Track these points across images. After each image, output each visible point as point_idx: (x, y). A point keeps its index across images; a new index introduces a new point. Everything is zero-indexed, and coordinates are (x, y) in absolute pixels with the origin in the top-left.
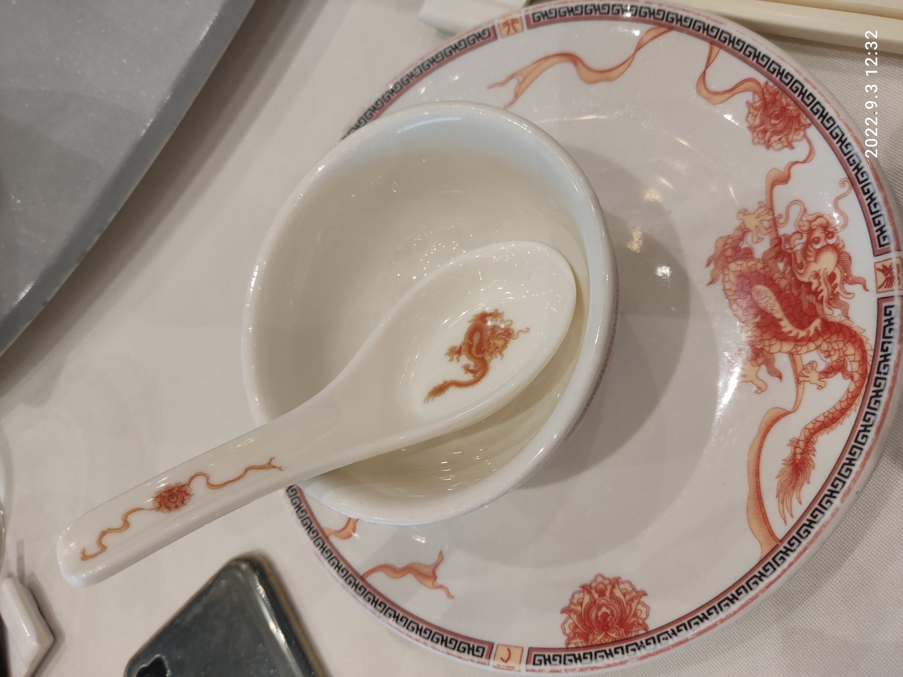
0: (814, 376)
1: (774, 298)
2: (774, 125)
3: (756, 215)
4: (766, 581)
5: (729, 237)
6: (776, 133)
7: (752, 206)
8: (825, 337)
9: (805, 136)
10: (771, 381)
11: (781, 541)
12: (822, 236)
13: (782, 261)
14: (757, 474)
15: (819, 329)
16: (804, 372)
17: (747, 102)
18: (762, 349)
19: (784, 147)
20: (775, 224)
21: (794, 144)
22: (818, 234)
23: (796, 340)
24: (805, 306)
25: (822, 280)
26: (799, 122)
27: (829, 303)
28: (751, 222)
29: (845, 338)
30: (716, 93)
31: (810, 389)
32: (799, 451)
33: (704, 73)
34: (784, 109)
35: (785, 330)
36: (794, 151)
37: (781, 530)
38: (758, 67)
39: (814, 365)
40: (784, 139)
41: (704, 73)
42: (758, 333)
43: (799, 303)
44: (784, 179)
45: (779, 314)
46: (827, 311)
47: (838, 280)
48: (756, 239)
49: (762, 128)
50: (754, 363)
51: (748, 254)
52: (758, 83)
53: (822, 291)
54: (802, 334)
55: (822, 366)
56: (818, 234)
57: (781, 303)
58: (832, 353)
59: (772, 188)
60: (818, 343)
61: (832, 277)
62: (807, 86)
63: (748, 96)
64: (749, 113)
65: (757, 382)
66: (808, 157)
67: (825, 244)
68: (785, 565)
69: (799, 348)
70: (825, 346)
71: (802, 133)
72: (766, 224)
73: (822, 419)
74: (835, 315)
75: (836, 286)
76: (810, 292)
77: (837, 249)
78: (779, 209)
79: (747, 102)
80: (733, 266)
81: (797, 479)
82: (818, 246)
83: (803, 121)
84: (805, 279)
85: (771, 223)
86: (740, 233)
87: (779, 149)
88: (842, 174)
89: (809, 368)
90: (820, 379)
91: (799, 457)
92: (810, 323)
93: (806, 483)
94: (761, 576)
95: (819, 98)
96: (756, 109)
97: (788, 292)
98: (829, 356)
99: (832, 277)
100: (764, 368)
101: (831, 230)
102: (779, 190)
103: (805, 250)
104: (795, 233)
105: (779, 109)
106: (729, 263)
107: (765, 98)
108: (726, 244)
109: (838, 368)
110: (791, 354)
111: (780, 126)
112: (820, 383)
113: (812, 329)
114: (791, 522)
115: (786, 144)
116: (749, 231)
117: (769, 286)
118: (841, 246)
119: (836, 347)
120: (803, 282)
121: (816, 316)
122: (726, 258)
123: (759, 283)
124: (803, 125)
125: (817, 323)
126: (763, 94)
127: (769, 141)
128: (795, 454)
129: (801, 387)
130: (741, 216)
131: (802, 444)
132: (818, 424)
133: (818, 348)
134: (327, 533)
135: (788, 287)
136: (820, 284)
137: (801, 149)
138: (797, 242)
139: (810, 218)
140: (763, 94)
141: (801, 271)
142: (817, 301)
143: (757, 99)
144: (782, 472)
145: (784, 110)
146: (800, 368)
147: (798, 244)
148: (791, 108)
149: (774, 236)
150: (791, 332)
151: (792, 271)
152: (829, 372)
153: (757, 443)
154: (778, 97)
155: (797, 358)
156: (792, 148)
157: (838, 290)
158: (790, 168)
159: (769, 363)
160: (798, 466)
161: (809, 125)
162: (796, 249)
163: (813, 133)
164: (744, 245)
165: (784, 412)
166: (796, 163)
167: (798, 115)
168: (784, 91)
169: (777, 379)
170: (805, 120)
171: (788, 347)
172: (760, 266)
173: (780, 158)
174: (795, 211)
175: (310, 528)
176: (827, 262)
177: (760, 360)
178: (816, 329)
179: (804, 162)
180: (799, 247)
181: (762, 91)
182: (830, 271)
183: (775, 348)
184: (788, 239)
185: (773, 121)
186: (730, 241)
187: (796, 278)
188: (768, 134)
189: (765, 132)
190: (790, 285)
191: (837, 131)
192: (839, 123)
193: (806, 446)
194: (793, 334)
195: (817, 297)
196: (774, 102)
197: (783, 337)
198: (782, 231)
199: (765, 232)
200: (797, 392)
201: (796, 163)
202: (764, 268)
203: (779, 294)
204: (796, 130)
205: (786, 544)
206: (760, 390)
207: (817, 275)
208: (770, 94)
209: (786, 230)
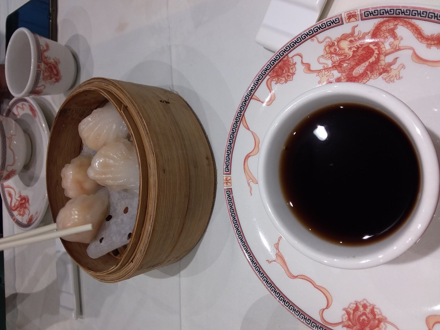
0: (396, 42)
1: (359, 67)
2: (286, 71)
7: (318, 79)
10: (398, 62)
12: (334, 48)
18: (383, 69)
19: (295, 67)
20: (327, 69)
23: (379, 54)
24: (363, 52)
25: (352, 46)
31: (403, 44)
34: (280, 68)
39: (391, 43)
40: (292, 67)
42: (375, 72)
44: (308, 67)
45: (367, 63)
47: (352, 39)
50: (390, 72)
52: (269, 79)
53: (357, 46)
54: (376, 52)
55: (391, 40)
56: (332, 50)
58: (385, 36)
63: (273, 83)
69: (383, 52)
71: (290, 59)
75: (355, 39)
76: (357, 51)
77: (339, 41)
78: (320, 67)
82: (338, 49)
84: (351, 53)
85: (326, 70)
87: (296, 69)
92: (372, 49)
96: (278, 80)
97: (357, 61)
98: (387, 37)
99: (351, 41)
100: (392, 67)
102: (312, 68)
104: (332, 60)
109: (392, 33)
110: (386, 55)
111: (286, 69)
112: (400, 39)
113: (374, 48)
127: (291, 73)
137: (297, 59)
138: (335, 59)
139: (325, 54)
141: (348, 56)
143: (275, 79)
146: (393, 50)
147: (336, 58)
152: (394, 36)
155: (388, 52)
159: (390, 65)
163: (290, 55)
170: (285, 59)
171: (382, 57)
172: (344, 74)
173: (299, 69)
174: (322, 60)
176: (345, 44)
177: (389, 69)
178: (374, 46)
181: (272, 77)
183: (382, 63)
184: (334, 62)
185: (284, 72)
188: (289, 74)
189: (288, 76)
194: (376, 56)
195: (360, 47)
196: (277, 72)
197: (378, 60)
198: (330, 66)
199: (330, 73)
201: (302, 60)
202: (345, 72)
203: (358, 64)
206: (403, 67)
207: (350, 48)
208: (273, 73)
209: (329, 63)
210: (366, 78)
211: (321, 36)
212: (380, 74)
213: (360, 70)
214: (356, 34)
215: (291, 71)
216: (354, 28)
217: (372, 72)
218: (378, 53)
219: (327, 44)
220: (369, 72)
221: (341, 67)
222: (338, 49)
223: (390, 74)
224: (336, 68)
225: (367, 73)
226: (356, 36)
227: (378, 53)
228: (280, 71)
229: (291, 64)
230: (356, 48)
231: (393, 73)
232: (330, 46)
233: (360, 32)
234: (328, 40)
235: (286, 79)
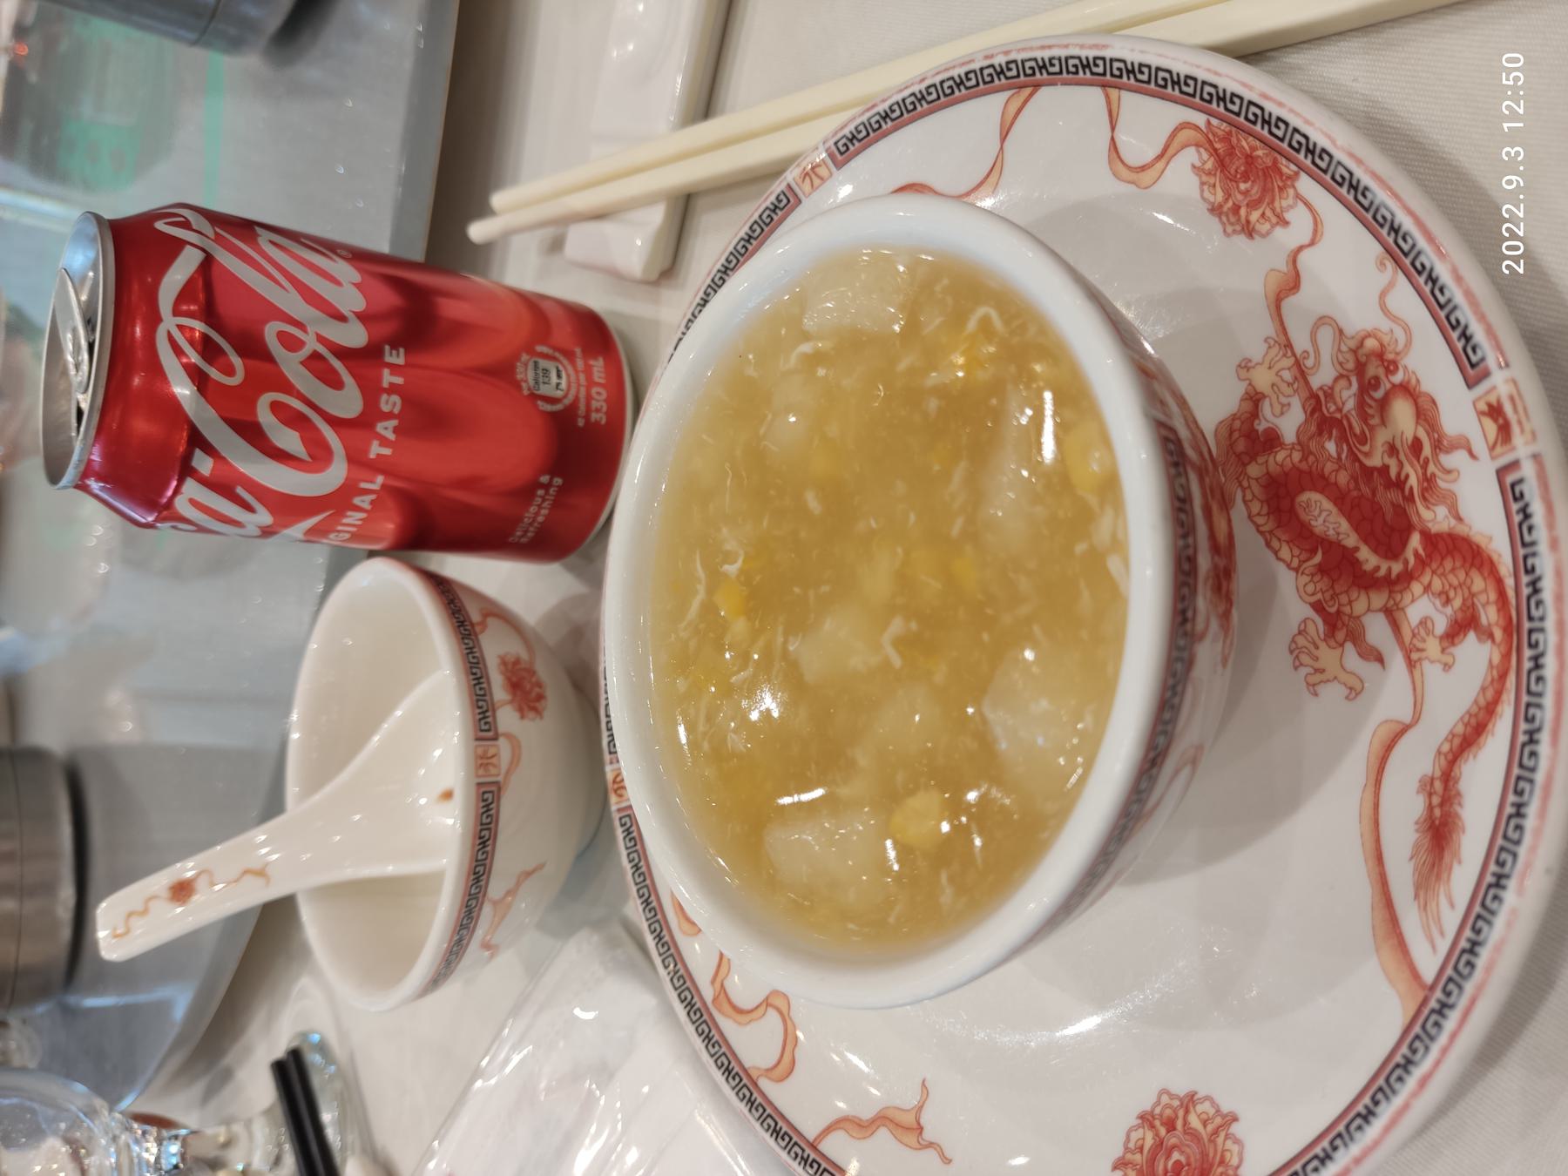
0: (1433, 647)
1: (1335, 510)
2: (1246, 193)
3: (1266, 364)
4: (1418, 1072)
5: (1234, 417)
6: (1252, 205)
8: (1434, 566)
9: (1298, 196)
11: (1432, 988)
13: (1330, 438)
14: (1379, 858)
15: (1421, 551)
16: (1415, 641)
17: (1194, 166)
18: (1338, 612)
19: (1273, 226)
20: (1301, 373)
21: (1288, 216)
22: (1373, 369)
25: (1402, 457)
26: (1281, 174)
27: (1425, 499)
28: (1263, 379)
29: (1464, 559)
30: (1143, 168)
31: (1431, 672)
32: (1436, 800)
33: (1113, 139)
34: (1250, 159)
35: (1368, 567)
36: (1291, 228)
37: (1429, 963)
38: (1186, 100)
39: (1429, 624)
40: (1269, 213)
41: (1113, 139)
42: (1323, 584)
43: (1377, 509)
44: (1292, 283)
45: (1351, 540)
46: (1426, 514)
47: (1427, 450)
48: (1277, 409)
49: (1230, 204)
51: (1272, 440)
52: (1196, 128)
53: (1407, 476)
54: (1397, 568)
55: (1441, 625)
57: (1349, 519)
58: (1452, 594)
59: (1278, 308)
60: (1426, 578)
61: (1416, 446)
62: (1269, 107)
64: (1203, 184)
65: (1343, 676)
66: (1315, 231)
67: (1388, 386)
68: (1443, 1039)
69: (1398, 597)
70: (1437, 584)
71: (1291, 192)
72: (1287, 376)
73: (1460, 729)
74: (1437, 518)
75: (1427, 461)
78: (1301, 342)
79: (1194, 166)
80: (1254, 470)
81: (1441, 858)
82: (1379, 394)
83: (1285, 170)
84: (1375, 461)
86: (1248, 406)
88: (1377, 248)
89: (1422, 632)
90: (1443, 651)
91: (1437, 812)
92: (1404, 543)
93: (1455, 865)
94: (1407, 1064)
95: (1295, 122)
97: (1355, 493)
98: (1448, 601)
99: (1416, 446)
100: (1349, 646)
101: (1390, 356)
103: (1361, 405)
104: (1336, 380)
105: (1242, 161)
106: (1245, 465)
107: (1216, 150)
108: (1231, 433)
109: (1464, 624)
111: (1255, 192)
114: (1444, 946)
115: (1274, 220)
116: (1264, 396)
117: (1322, 492)
118: (1413, 381)
119: (1455, 582)
120: (1374, 469)
121: (1408, 528)
122: (1238, 456)
123: (1302, 490)
124: (1289, 177)
125: (1415, 541)
126: (1210, 142)
127: (1248, 222)
128: (1430, 808)
129: (1417, 673)
130: (1243, 373)
131: (1438, 785)
132: (1457, 741)
133: (1427, 589)
134: (754, 1074)
135: (1352, 486)
136: (1401, 465)
137: (1299, 220)
138: (1345, 394)
140: (1210, 142)
141: (1366, 448)
142: (1404, 497)
143: (1205, 156)
144: (1417, 847)
145: (1252, 158)
147: (1348, 397)
148: (1260, 153)
149: (1305, 394)
150: (1377, 568)
151: (1350, 449)
152: (1454, 633)
153: (1369, 796)
154: (1234, 140)
155: (1398, 615)
156: (1286, 223)
157: (1431, 468)
158: (1295, 262)
159: (1356, 637)
160: (1439, 832)
161: (1297, 174)
162: (1345, 410)
163: (1306, 185)
164: (1261, 427)
165: (1398, 728)
166: (1301, 248)
167: (1275, 162)
168: (1239, 127)
169: (1377, 665)
170: (1288, 168)
171: (1379, 599)
172: (1297, 456)
175: (727, 1071)
177: (1340, 635)
178: (1416, 554)
179: (1312, 243)
180: (1350, 404)
181: (1207, 141)
182: (1409, 436)
184: (1329, 393)
185: (1243, 186)
186: (1237, 424)
187: (1362, 464)
188: (1243, 212)
189: (1236, 209)
190: (1354, 478)
191: (1341, 170)
192: (1339, 155)
193: (1446, 788)
194: (1382, 572)
195: (1403, 490)
196: (1231, 151)
197: (1368, 582)
199: (1289, 391)
200: (1413, 683)
202: (1304, 458)
204: (1281, 189)
205: (1438, 994)
207: (1392, 449)
208: (1222, 140)
209: (1323, 376)
210: (1296, 551)
211: (1407, 301)
212: (1318, 607)
213: (1323, 515)
214: (1448, 460)
215: (1255, 216)
216: (1465, 445)
217: (1322, 570)
218: (1394, 575)
219: (1386, 339)
220: (1318, 558)
221: (1320, 432)
222: (1379, 394)
223: (1323, 645)
224: (1312, 413)
225: (1313, 552)
226: (1438, 463)
227: (1394, 575)
228: (1238, 165)
229: (1277, 204)
230: (1399, 474)
231: (1327, 656)
232: (1380, 355)
233: (1454, 475)
234: (1400, 334)
235: (1221, 206)
